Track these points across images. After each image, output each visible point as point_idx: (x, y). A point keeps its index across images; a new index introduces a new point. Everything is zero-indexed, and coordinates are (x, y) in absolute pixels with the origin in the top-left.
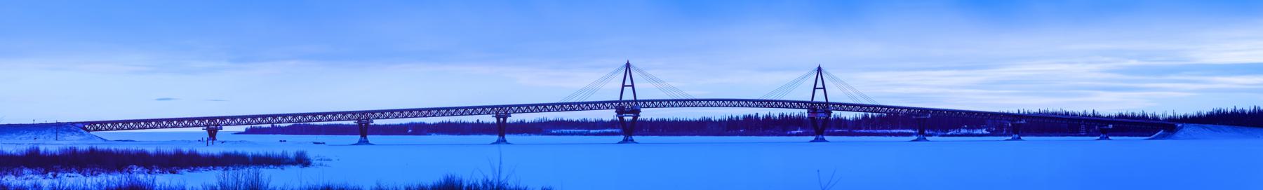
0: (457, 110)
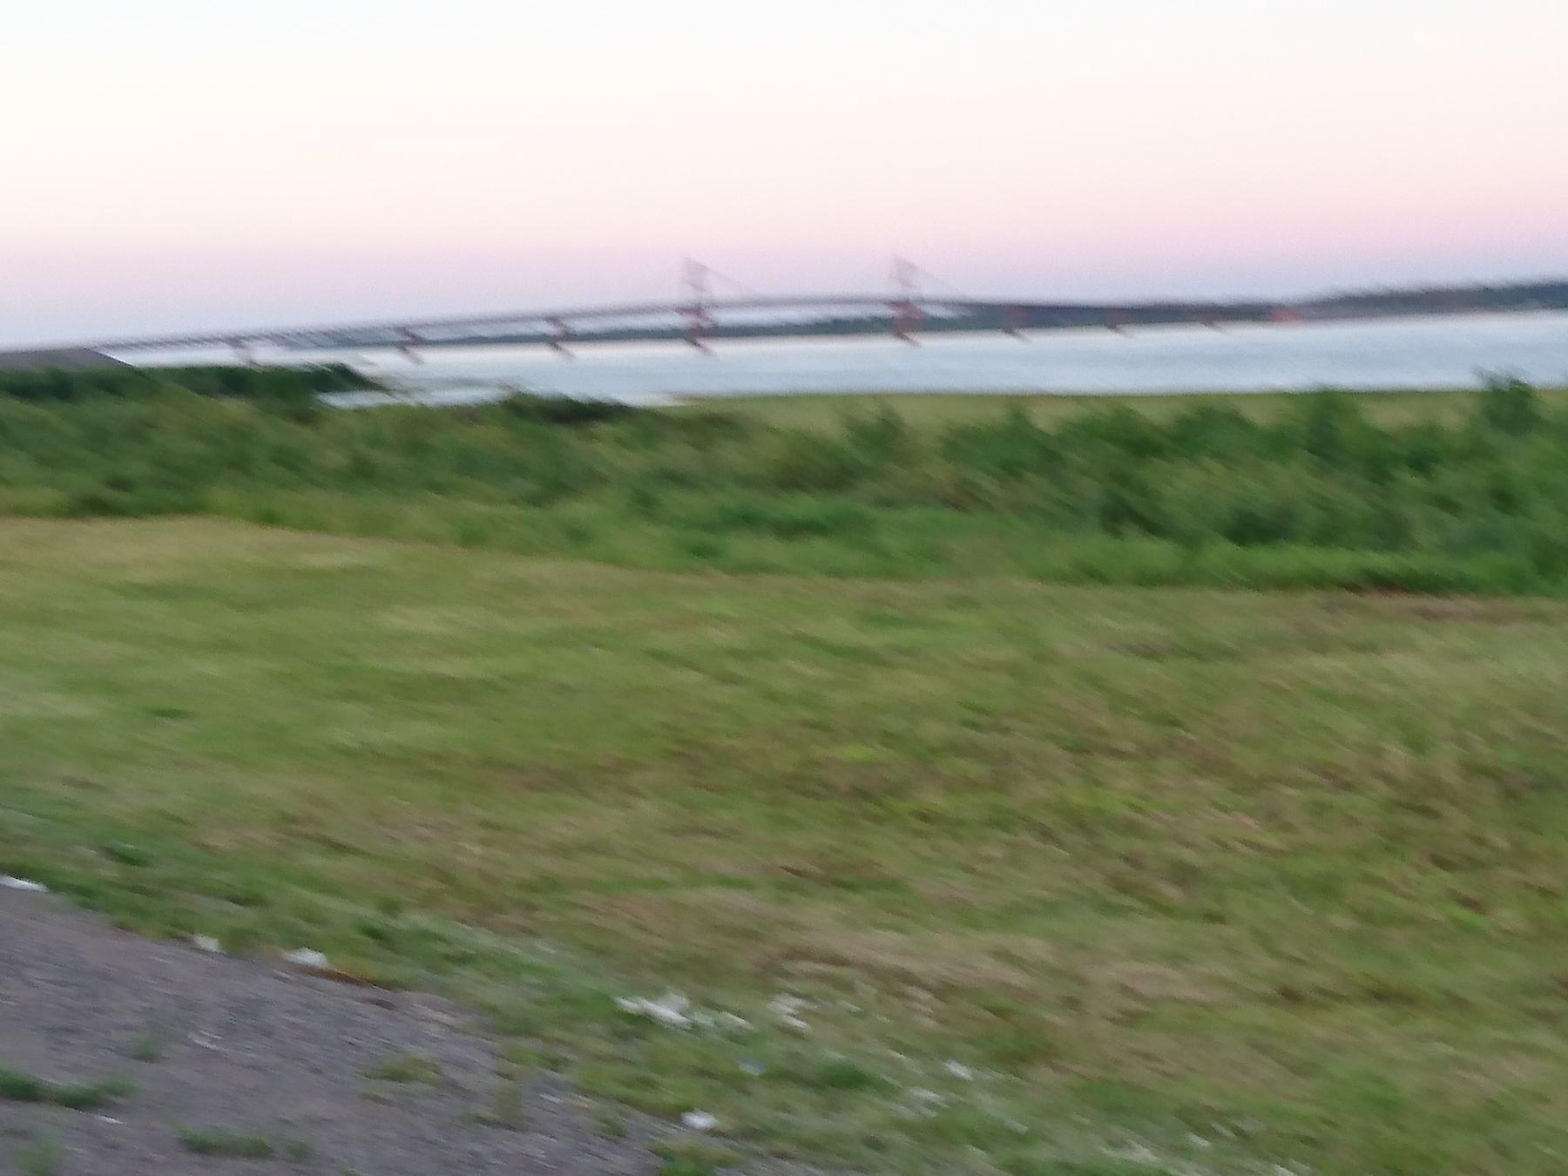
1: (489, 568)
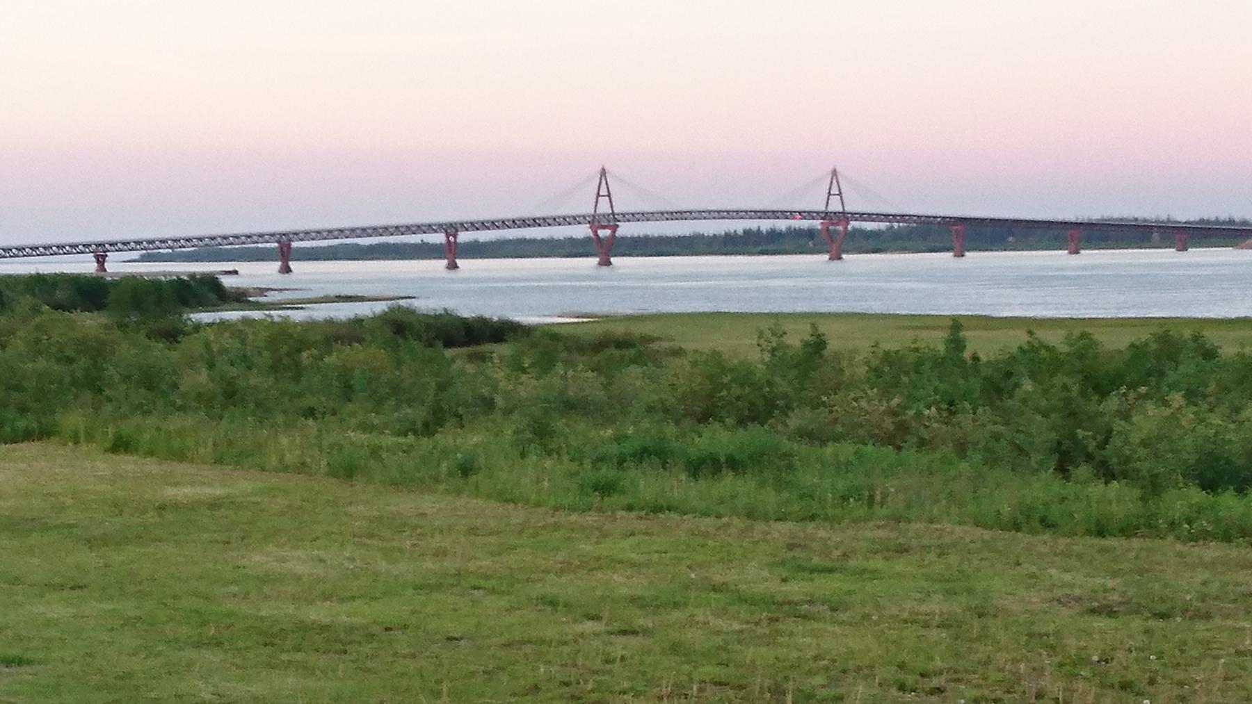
0: (398, 230)
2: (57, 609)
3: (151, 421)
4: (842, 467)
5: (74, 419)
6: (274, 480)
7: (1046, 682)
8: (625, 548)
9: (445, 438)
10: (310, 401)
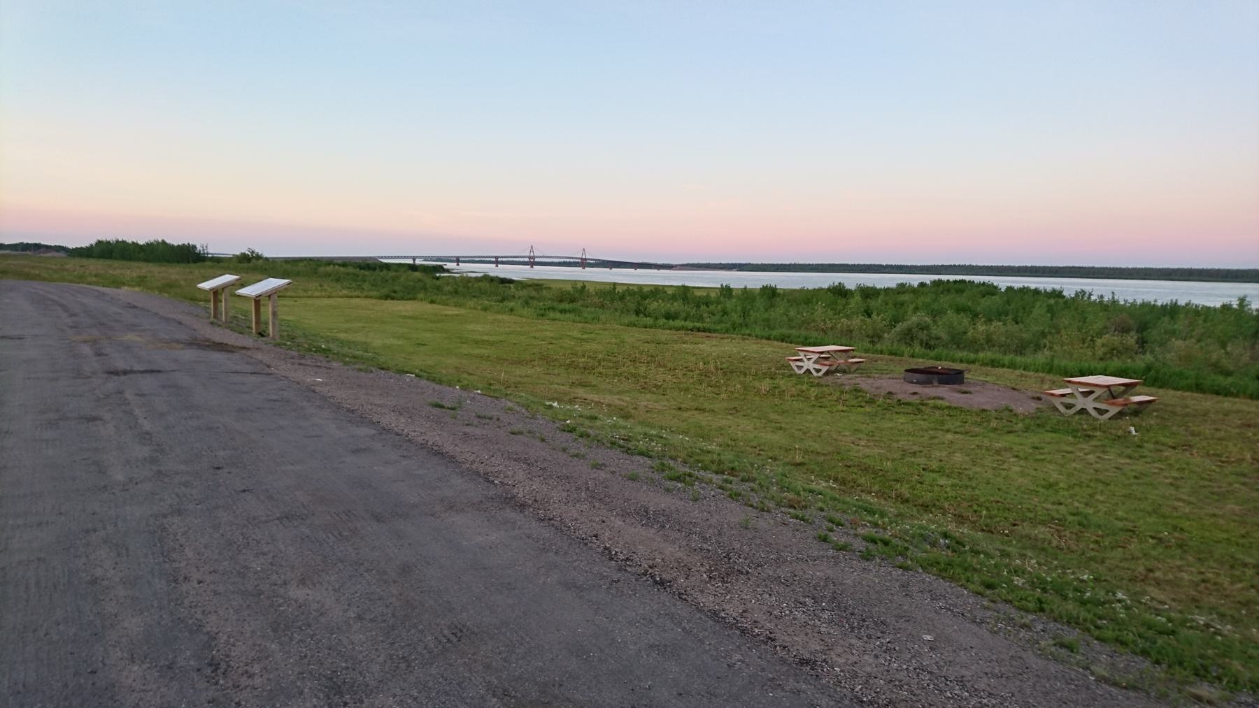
1: (490, 316)
2: (428, 335)
3: (439, 297)
4: (592, 313)
5: (421, 296)
6: (469, 311)
7: (637, 355)
8: (548, 327)
9: (505, 303)
10: (474, 294)
